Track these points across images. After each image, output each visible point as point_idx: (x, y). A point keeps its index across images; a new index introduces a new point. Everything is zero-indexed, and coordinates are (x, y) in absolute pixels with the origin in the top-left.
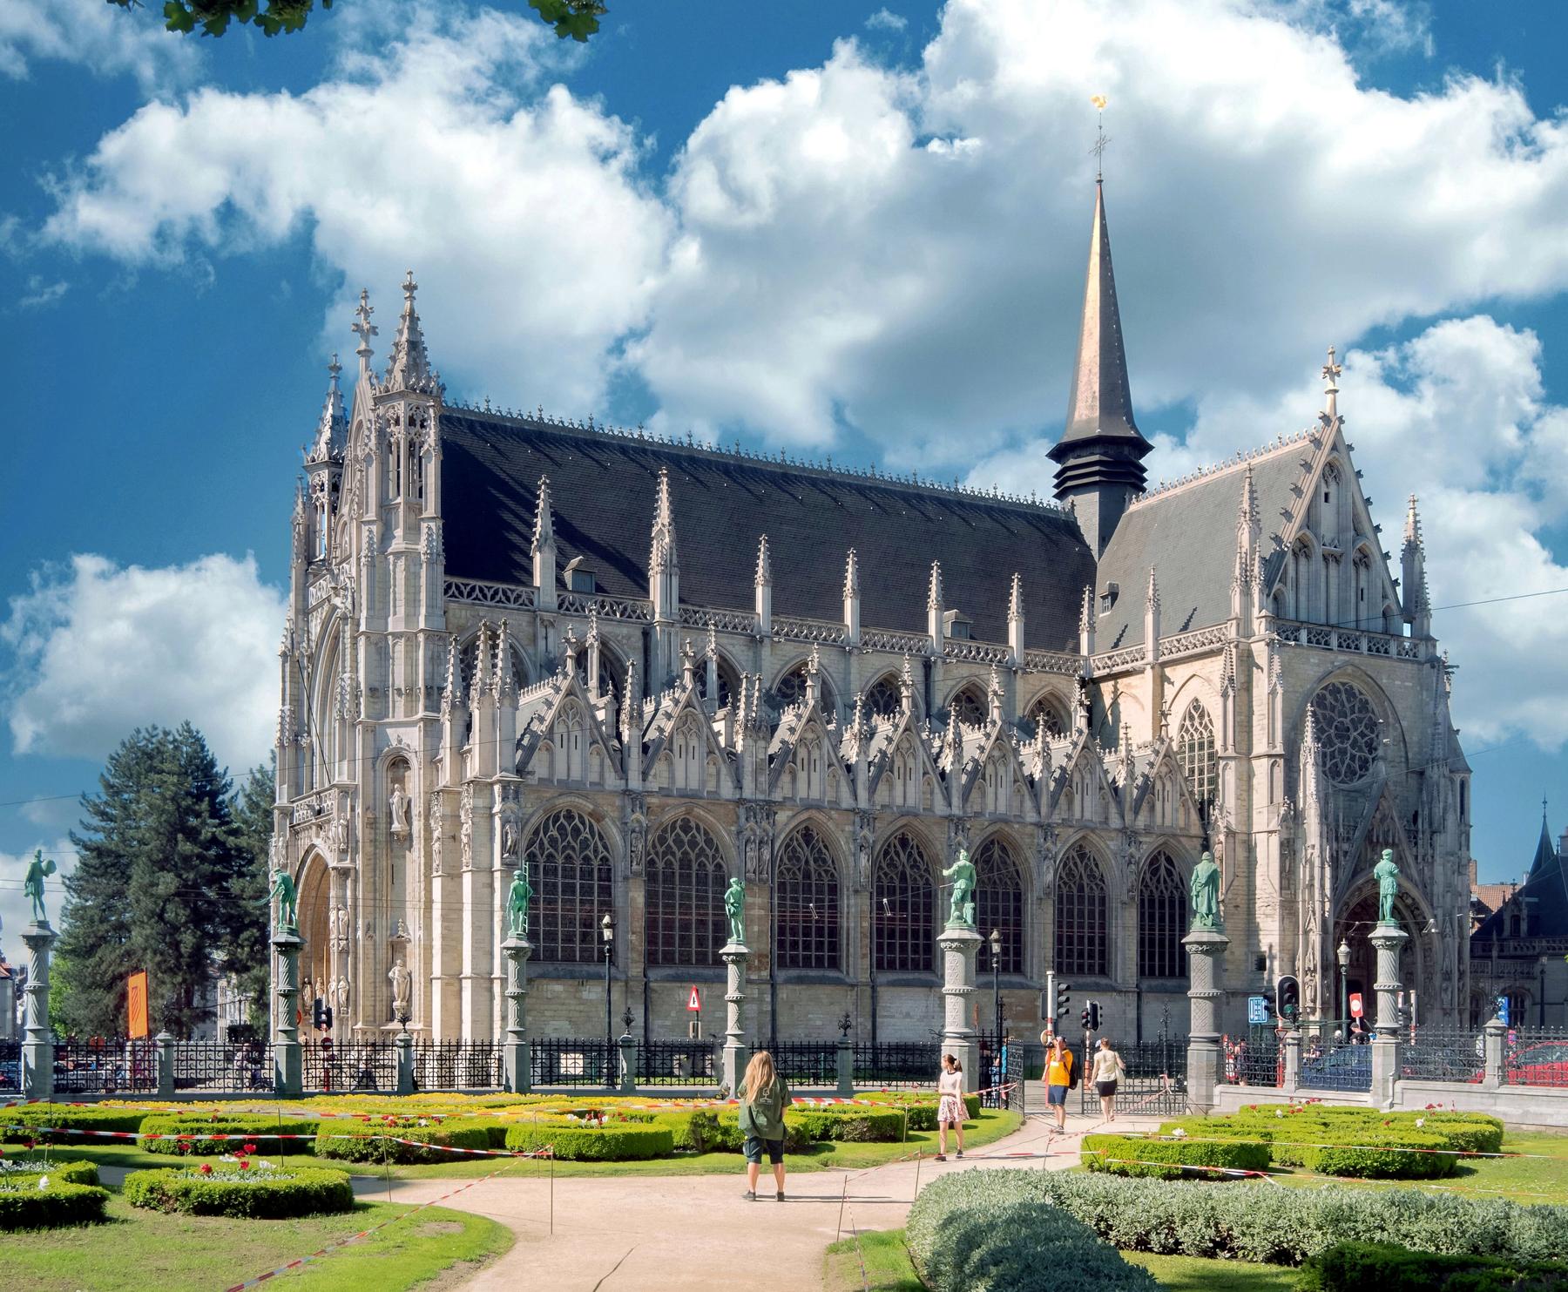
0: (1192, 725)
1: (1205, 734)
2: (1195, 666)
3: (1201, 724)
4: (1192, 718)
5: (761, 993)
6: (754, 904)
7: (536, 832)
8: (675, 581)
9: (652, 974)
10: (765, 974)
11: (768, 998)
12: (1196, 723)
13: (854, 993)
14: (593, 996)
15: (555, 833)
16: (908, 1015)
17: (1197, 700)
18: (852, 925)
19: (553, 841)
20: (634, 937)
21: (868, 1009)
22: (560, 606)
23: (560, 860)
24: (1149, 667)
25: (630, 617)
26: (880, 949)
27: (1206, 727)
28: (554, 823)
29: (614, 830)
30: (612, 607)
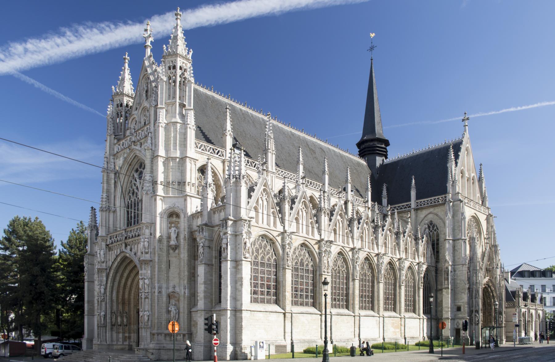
1: (435, 233)
2: (431, 210)
3: (433, 229)
12: (431, 229)
15: (258, 246)
17: (431, 221)
23: (260, 257)
24: (413, 210)
27: (435, 230)
30: (251, 163)
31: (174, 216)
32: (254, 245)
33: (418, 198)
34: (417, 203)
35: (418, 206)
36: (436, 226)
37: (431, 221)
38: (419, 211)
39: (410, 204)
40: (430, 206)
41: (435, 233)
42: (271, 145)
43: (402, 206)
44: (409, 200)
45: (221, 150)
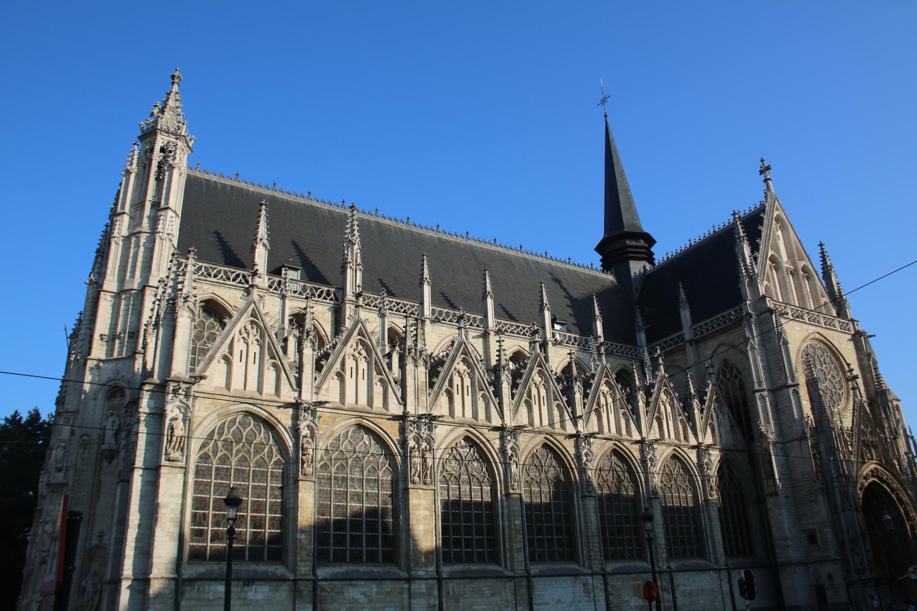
0: (725, 377)
2: (722, 338)
3: (731, 375)
4: (724, 373)
5: (430, 588)
6: (419, 505)
7: (211, 436)
8: (359, 274)
9: (321, 573)
10: (432, 569)
11: (436, 593)
12: (728, 375)
13: (512, 584)
14: (259, 597)
15: (230, 436)
16: (559, 601)
17: (725, 360)
18: (506, 523)
19: (228, 445)
20: (303, 536)
21: (525, 597)
22: (270, 287)
25: (325, 298)
26: (531, 545)
27: (736, 377)
28: (229, 428)
29: (287, 436)
31: (119, 395)
32: (221, 434)
33: (695, 319)
34: (695, 329)
35: (697, 335)
36: (737, 368)
37: (725, 360)
38: (702, 346)
39: (683, 334)
40: (717, 331)
41: (736, 382)
42: (355, 254)
43: (670, 340)
44: (679, 327)
45: (242, 272)
